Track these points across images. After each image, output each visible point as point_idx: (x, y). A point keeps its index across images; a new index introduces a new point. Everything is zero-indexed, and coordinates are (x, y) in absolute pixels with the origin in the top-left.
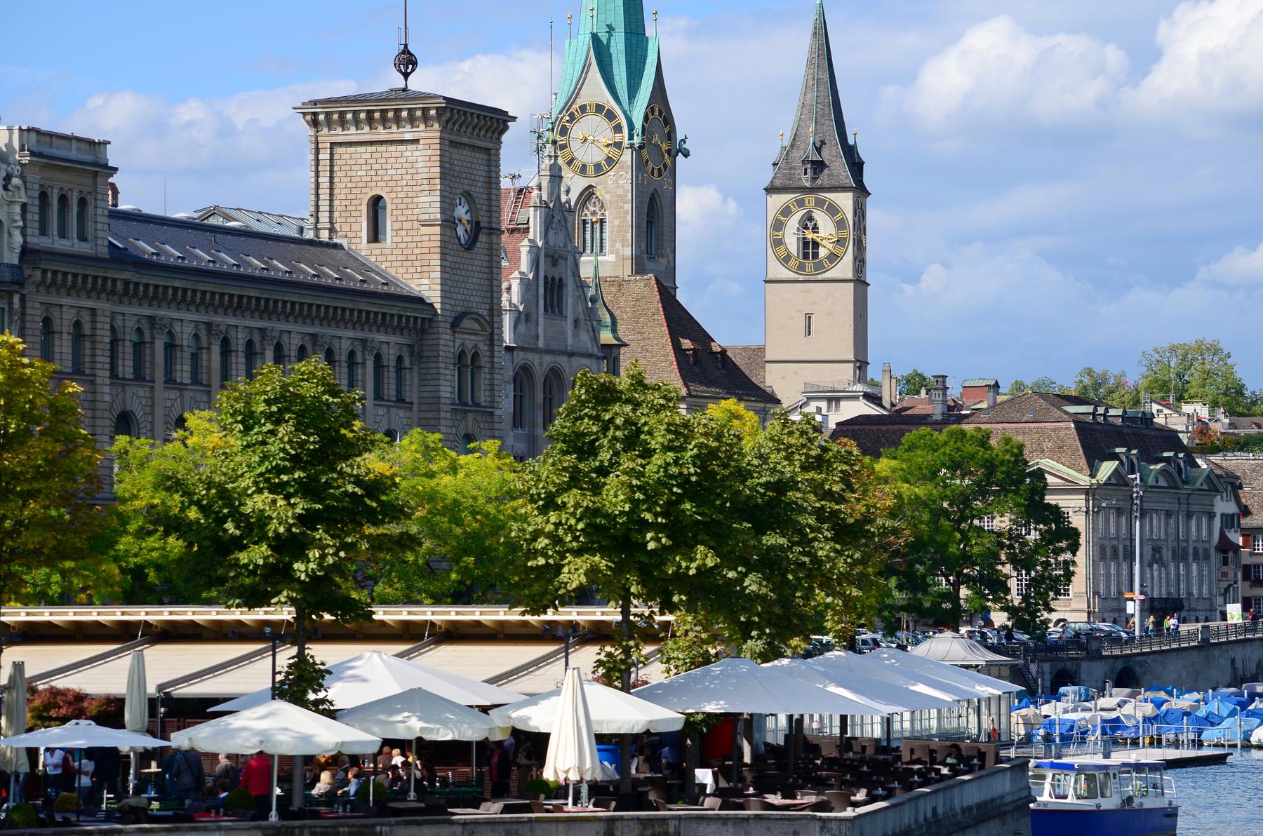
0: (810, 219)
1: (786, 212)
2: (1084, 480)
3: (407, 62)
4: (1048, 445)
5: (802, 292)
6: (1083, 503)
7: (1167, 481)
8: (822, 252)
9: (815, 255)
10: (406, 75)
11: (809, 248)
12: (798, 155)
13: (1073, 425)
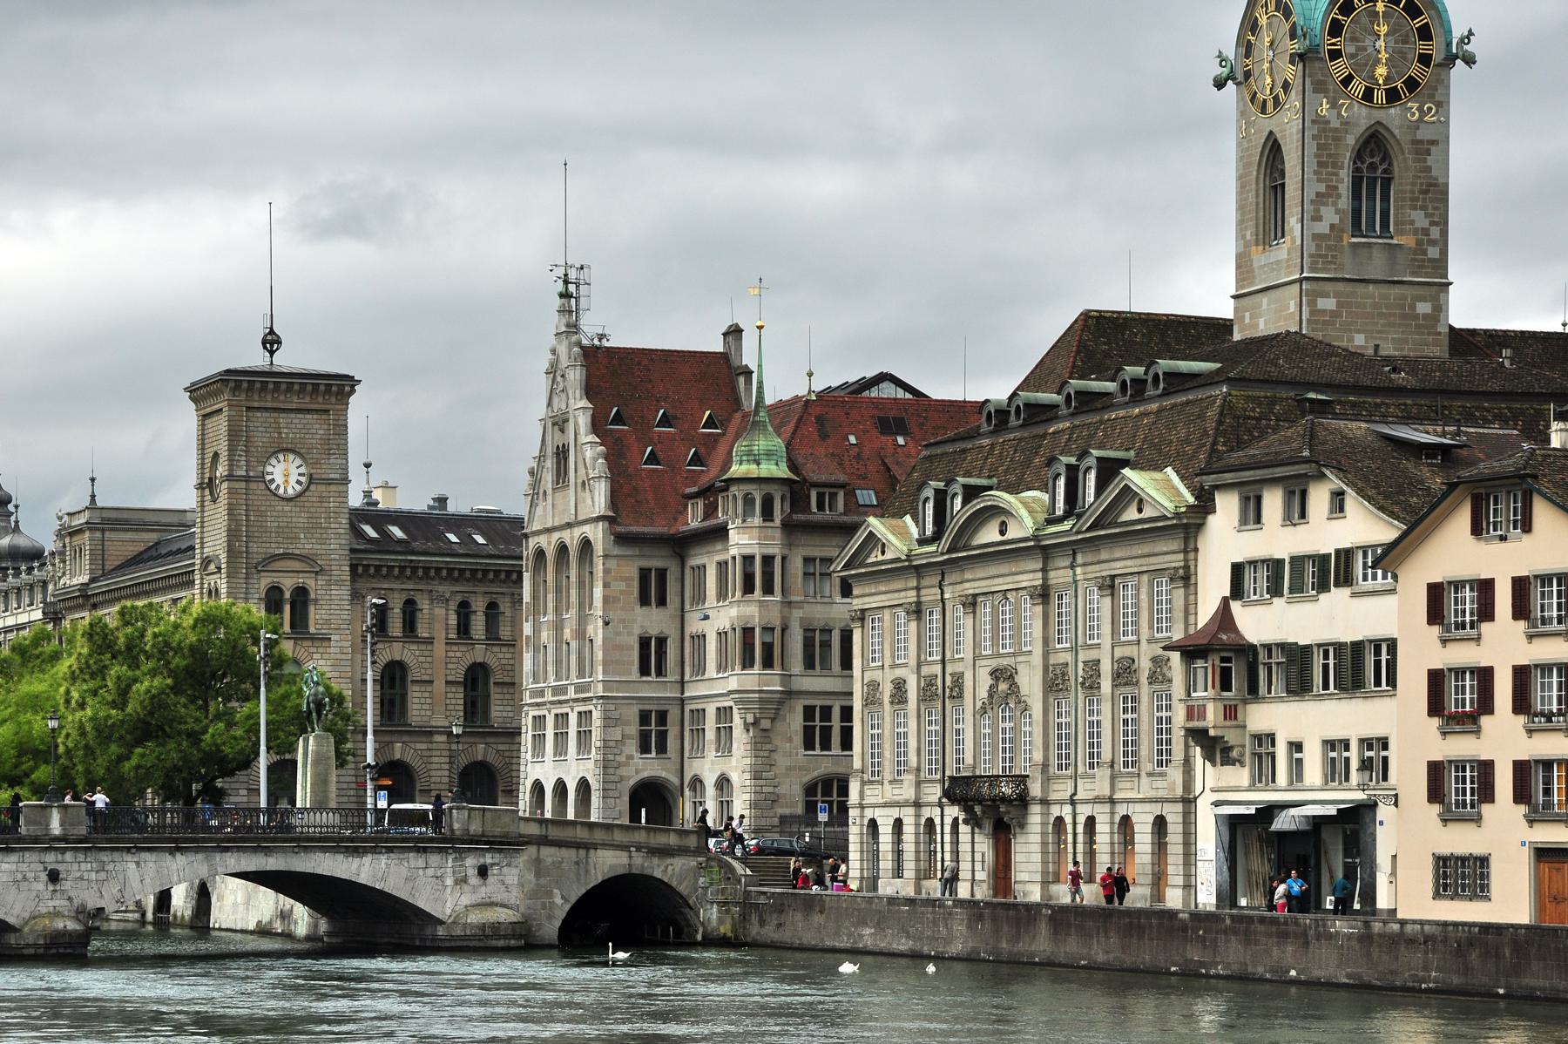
3: (271, 342)
10: (272, 353)
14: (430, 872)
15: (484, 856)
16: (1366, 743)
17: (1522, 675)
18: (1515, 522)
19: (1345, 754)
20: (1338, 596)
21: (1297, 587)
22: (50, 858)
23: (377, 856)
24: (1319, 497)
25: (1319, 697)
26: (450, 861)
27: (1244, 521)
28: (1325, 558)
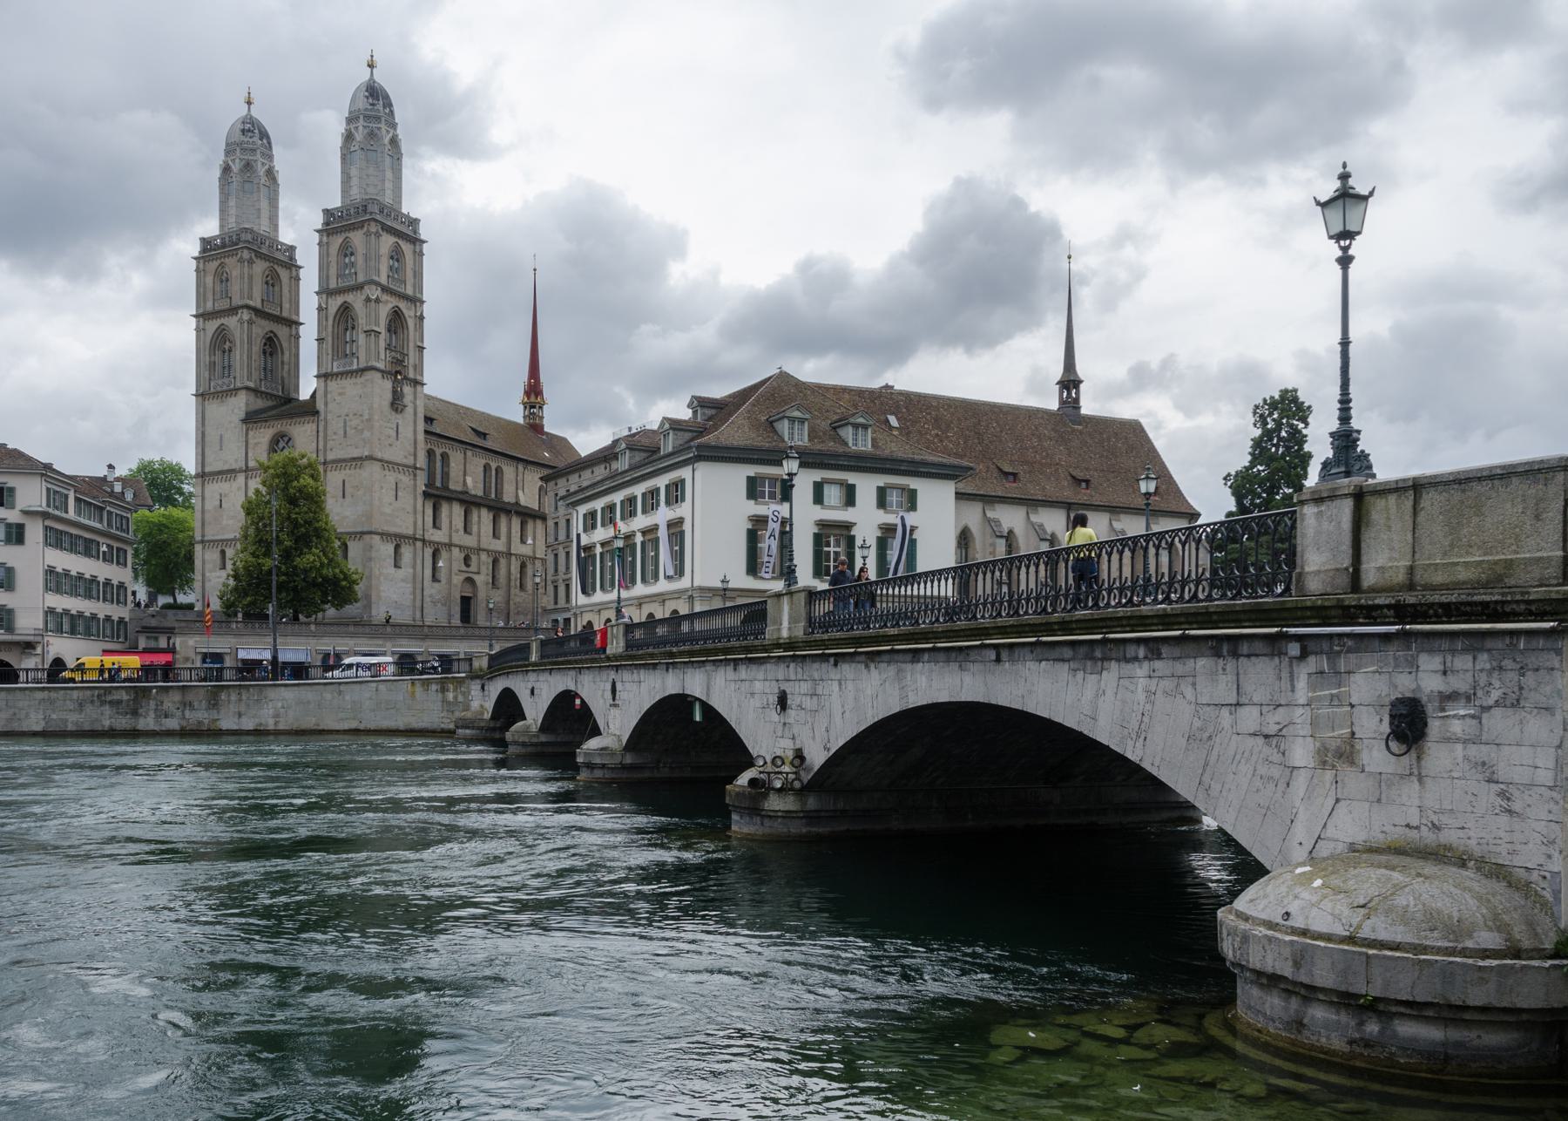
14: (1249, 718)
15: (1414, 667)
22: (780, 671)
23: (1127, 668)
26: (1302, 683)
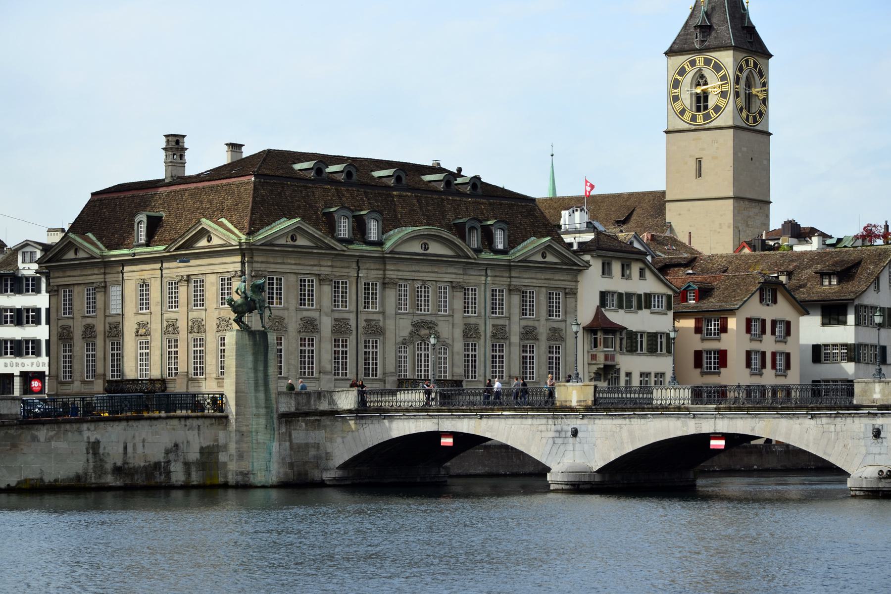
0: (702, 76)
1: (682, 72)
2: (236, 237)
4: (229, 203)
5: (694, 140)
6: (238, 267)
7: (451, 249)
8: (711, 103)
9: (706, 108)
11: (701, 100)
12: (694, 22)
13: (253, 179)
16: (641, 376)
17: (774, 355)
18: (769, 299)
19: (656, 379)
20: (645, 312)
21: (629, 306)
24: (635, 268)
25: (639, 354)
27: (603, 273)
28: (639, 296)
